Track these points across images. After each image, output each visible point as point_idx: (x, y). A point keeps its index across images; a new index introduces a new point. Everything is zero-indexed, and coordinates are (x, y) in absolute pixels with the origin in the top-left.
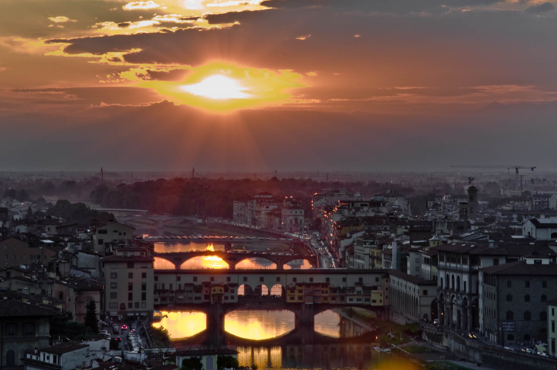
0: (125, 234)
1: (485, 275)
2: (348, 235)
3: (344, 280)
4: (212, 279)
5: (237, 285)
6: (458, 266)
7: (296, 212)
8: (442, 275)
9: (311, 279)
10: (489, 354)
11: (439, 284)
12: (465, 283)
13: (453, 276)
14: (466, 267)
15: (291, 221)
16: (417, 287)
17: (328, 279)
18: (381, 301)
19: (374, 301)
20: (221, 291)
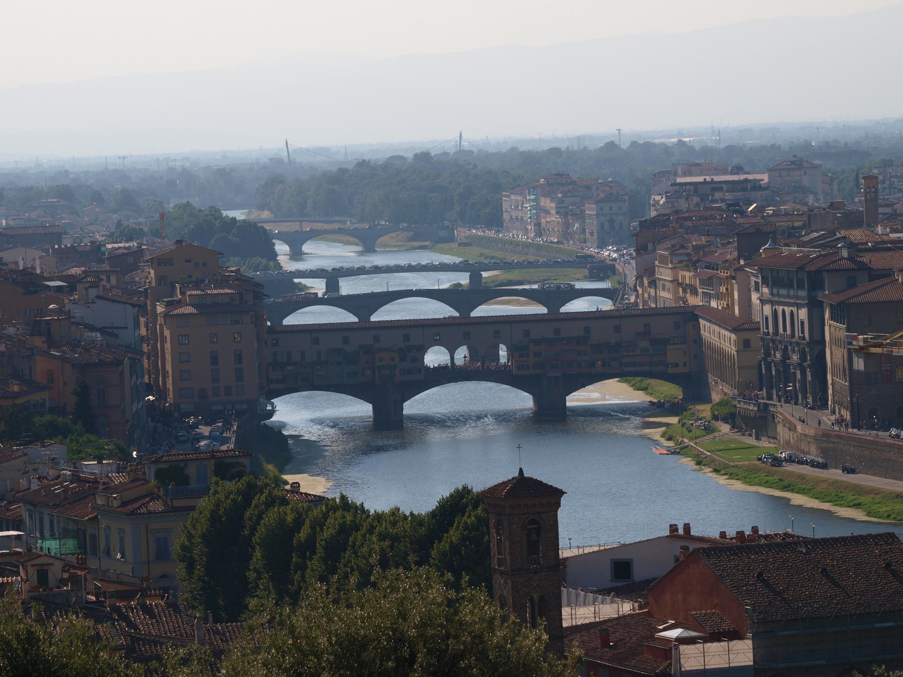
0: (205, 264)
1: (832, 307)
2: (650, 246)
3: (618, 329)
4: (377, 339)
5: (423, 350)
6: (791, 292)
7: (611, 208)
8: (767, 310)
9: (557, 331)
10: (832, 445)
11: (763, 329)
12: (802, 323)
13: (784, 311)
14: (803, 293)
15: (602, 226)
16: (733, 337)
17: (587, 330)
18: (685, 365)
19: (677, 365)
20: (393, 359)
